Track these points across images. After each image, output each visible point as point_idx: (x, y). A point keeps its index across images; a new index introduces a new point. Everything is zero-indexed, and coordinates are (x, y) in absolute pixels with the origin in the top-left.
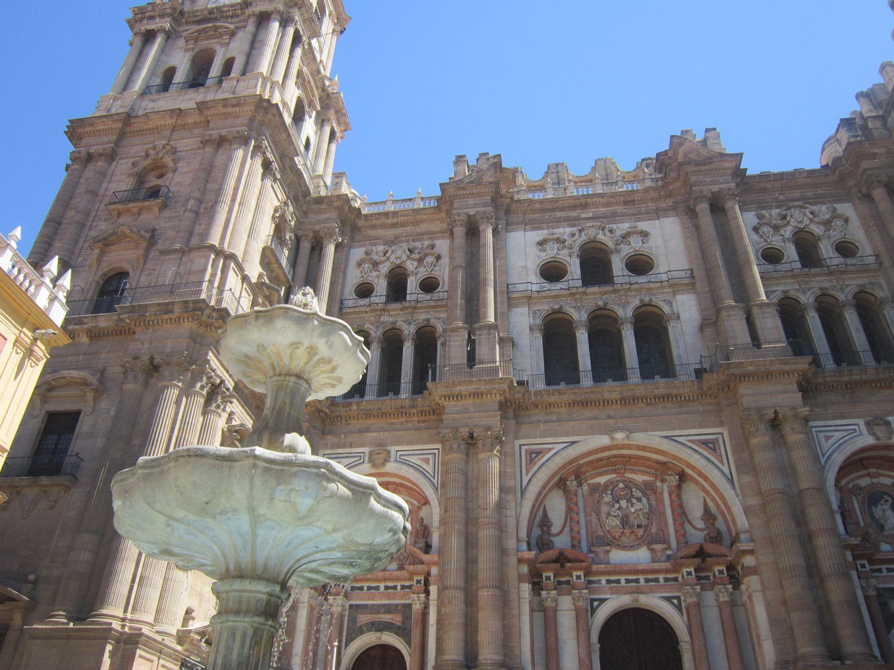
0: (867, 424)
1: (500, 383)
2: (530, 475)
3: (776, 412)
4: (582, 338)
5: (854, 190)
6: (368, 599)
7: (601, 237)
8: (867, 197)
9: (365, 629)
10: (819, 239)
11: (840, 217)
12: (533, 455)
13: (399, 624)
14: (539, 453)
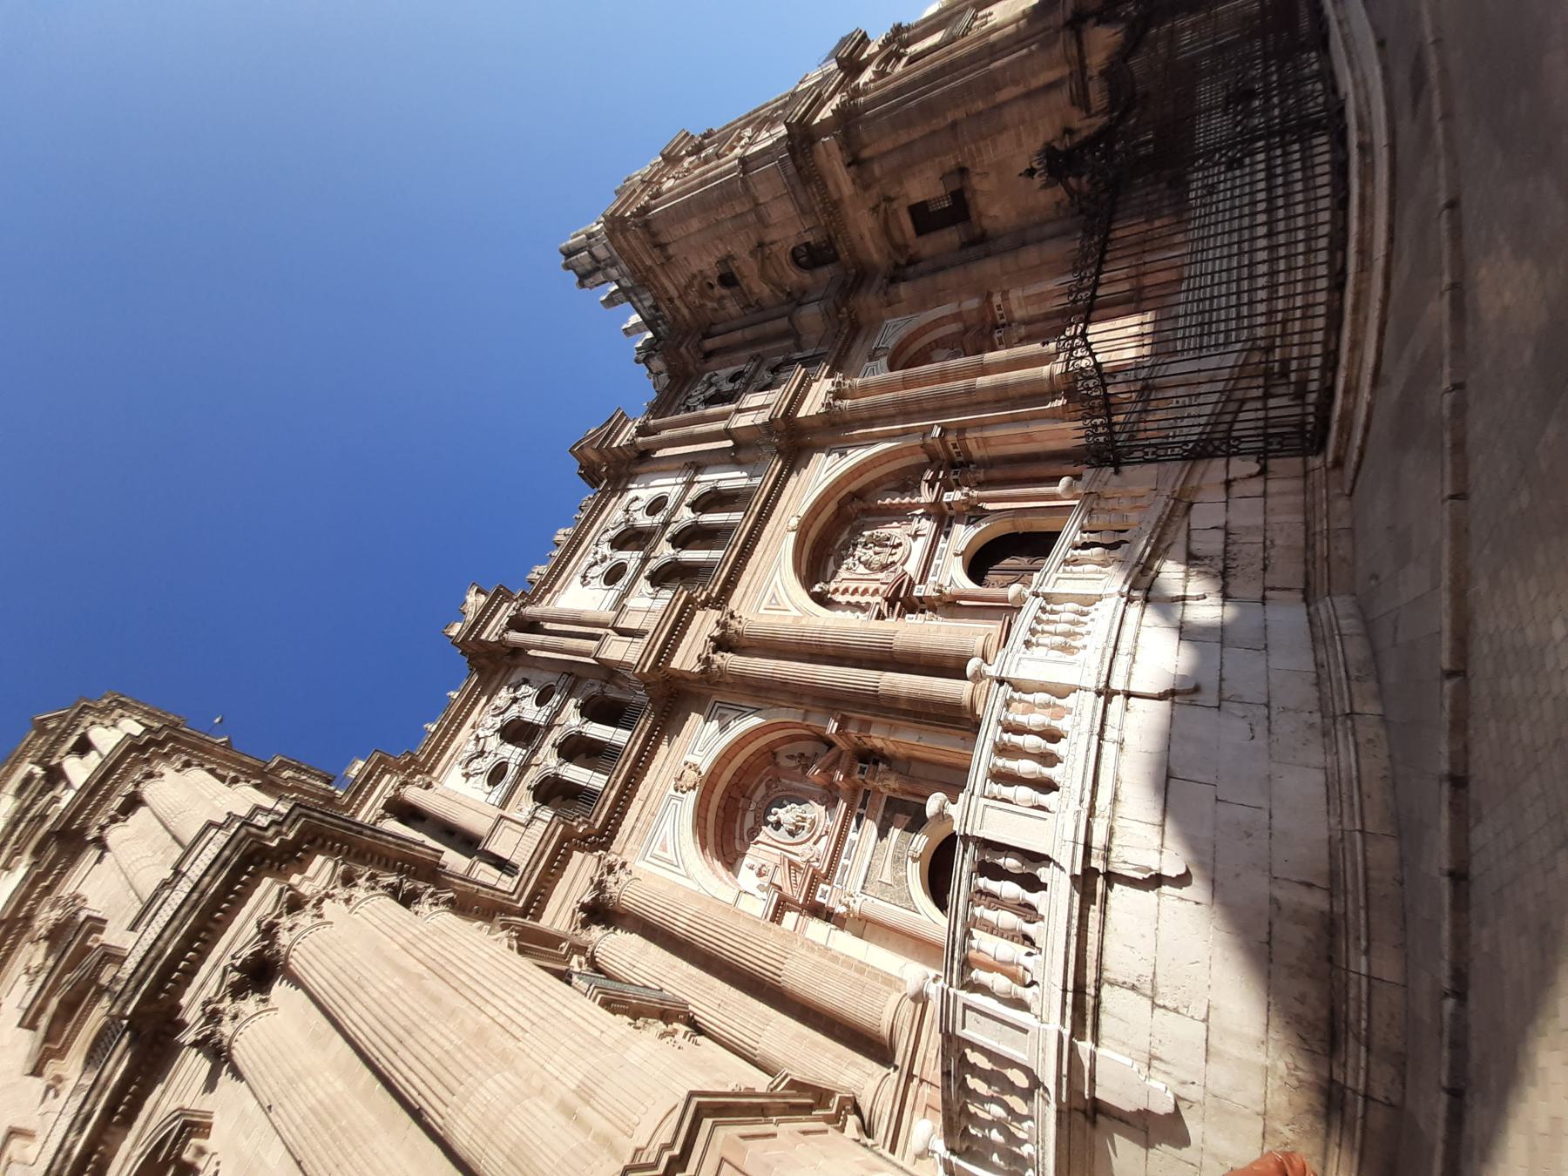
0: (870, 360)
1: (678, 600)
2: (790, 607)
3: (830, 392)
4: (688, 555)
5: (697, 365)
6: (862, 861)
7: (612, 533)
8: (709, 355)
9: (901, 874)
10: (718, 391)
11: (711, 377)
12: (774, 601)
13: (909, 818)
14: (774, 595)
